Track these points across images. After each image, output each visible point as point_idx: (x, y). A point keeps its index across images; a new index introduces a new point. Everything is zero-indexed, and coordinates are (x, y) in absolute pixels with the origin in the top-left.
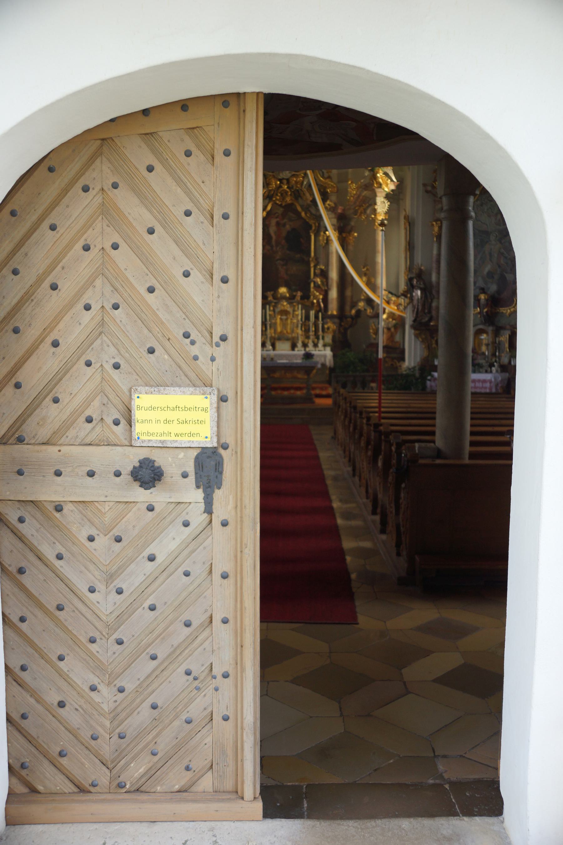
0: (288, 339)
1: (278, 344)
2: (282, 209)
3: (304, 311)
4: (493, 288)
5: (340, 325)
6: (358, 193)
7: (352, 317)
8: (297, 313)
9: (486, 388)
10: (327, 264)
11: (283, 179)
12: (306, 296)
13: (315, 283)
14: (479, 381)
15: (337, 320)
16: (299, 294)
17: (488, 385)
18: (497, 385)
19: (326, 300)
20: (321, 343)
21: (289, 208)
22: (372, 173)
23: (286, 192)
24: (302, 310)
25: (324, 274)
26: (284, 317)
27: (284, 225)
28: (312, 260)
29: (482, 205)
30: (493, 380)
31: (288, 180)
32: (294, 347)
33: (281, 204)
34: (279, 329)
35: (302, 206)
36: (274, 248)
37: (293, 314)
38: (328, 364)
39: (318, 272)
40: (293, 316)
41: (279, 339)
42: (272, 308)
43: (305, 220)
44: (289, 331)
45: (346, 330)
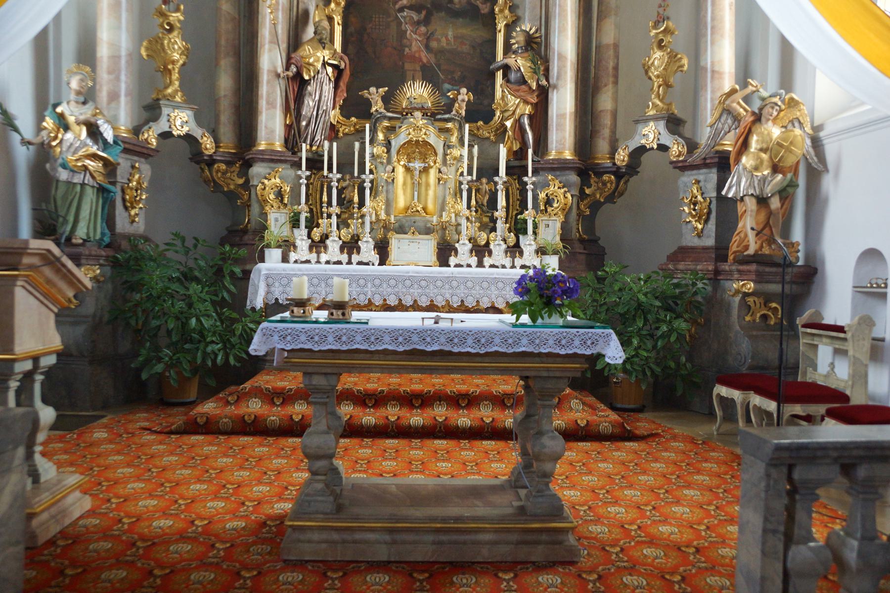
0: (428, 231)
1: (398, 245)
3: (476, 149)
5: (582, 195)
7: (618, 173)
8: (456, 152)
10: (546, 21)
13: (506, 68)
15: (574, 178)
16: (464, 95)
20: (528, 244)
24: (471, 146)
26: (417, 165)
28: (501, 11)
32: (445, 253)
34: (401, 202)
37: (445, 155)
39: (518, 40)
40: (445, 162)
41: (401, 230)
42: (381, 136)
44: (430, 206)
45: (596, 206)
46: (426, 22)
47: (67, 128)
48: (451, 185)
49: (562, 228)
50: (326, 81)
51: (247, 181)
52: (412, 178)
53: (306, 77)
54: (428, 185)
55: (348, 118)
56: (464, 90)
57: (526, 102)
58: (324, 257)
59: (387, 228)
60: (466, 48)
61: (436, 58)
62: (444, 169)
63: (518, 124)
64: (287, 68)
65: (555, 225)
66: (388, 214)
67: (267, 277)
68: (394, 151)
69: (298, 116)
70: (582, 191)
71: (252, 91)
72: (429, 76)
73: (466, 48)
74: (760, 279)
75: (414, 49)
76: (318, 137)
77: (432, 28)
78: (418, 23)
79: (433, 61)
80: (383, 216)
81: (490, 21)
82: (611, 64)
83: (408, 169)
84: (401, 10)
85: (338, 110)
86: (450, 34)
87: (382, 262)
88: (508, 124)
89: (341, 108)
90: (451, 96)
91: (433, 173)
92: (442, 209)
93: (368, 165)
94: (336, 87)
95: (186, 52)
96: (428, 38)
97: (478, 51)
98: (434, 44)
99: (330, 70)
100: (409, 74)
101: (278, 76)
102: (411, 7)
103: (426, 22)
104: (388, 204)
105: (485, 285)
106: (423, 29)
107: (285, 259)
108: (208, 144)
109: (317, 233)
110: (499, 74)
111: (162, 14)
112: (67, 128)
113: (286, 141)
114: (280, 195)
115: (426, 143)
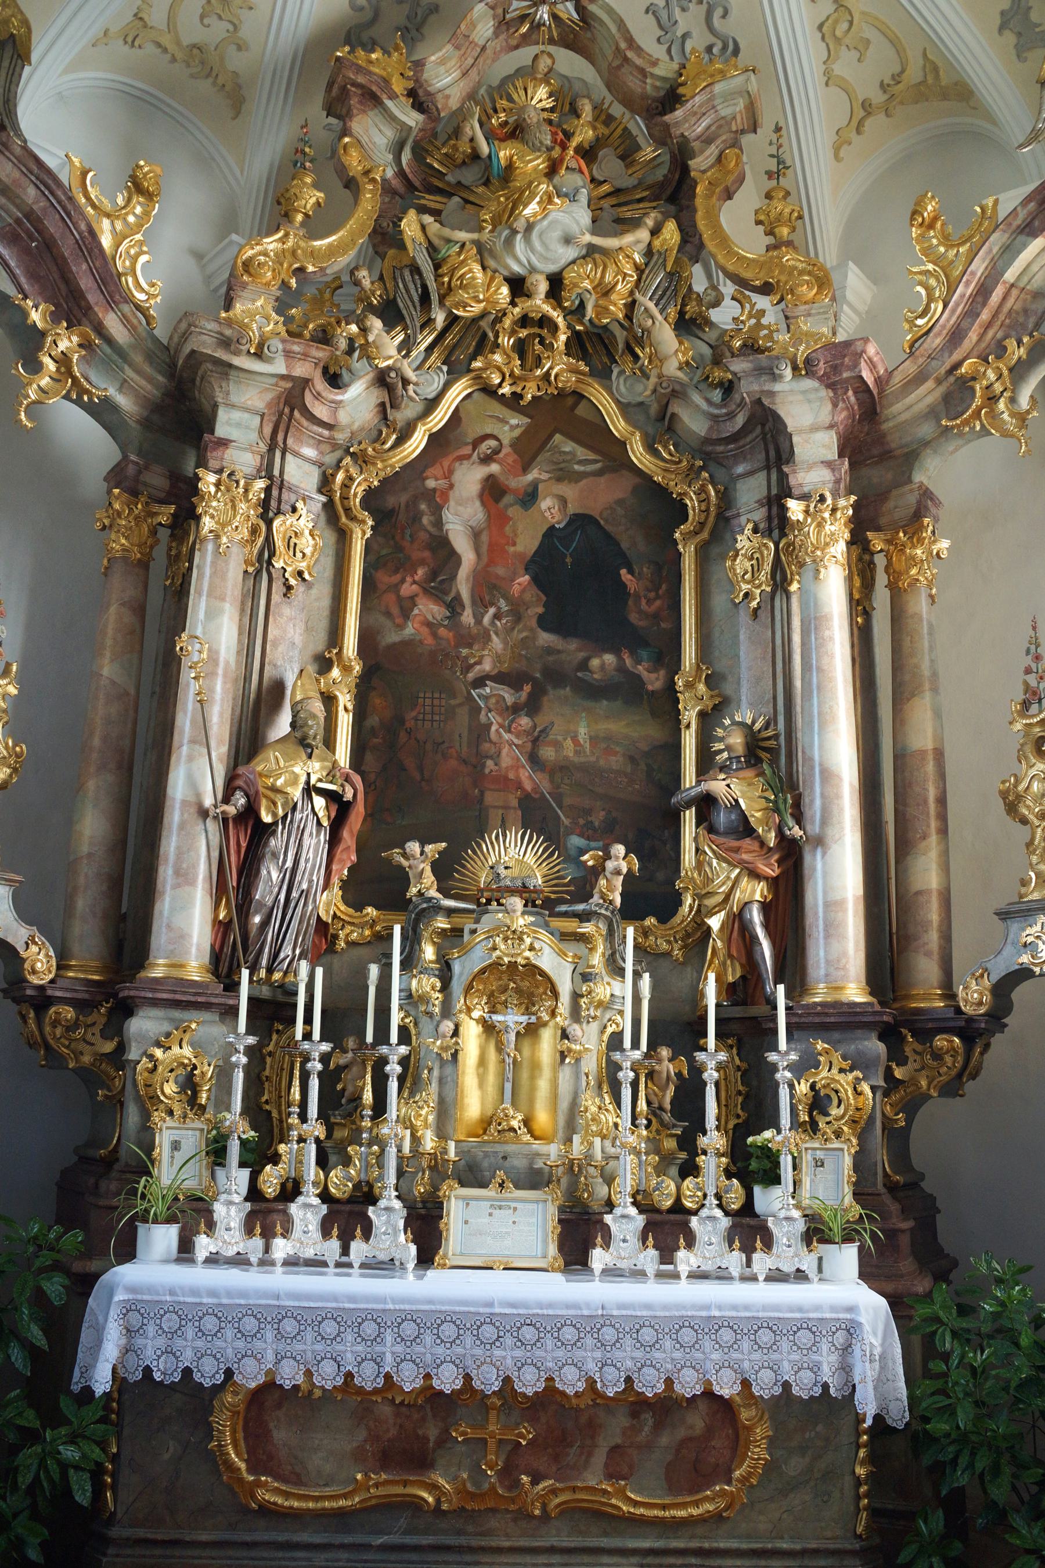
5: (892, 1083)
13: (706, 804)
24: (637, 975)
26: (513, 1019)
27: (530, 497)
28: (690, 686)
33: (517, 396)
35: (625, 408)
36: (467, 617)
37: (576, 996)
38: (868, 1405)
42: (429, 952)
43: (647, 478)
44: (542, 1118)
45: (912, 1107)
46: (532, 706)
48: (591, 1064)
49: (856, 1167)
50: (311, 826)
51: (122, 1048)
52: (500, 1048)
53: (267, 819)
54: (535, 1066)
55: (358, 906)
56: (620, 849)
57: (755, 875)
58: (281, 1248)
59: (437, 1167)
60: (616, 762)
61: (552, 781)
62: (575, 1030)
63: (738, 922)
64: (226, 800)
66: (442, 1135)
67: (129, 1308)
68: (457, 986)
69: (244, 905)
70: (889, 1075)
73: (616, 762)
75: (506, 761)
76: (287, 951)
77: (542, 720)
78: (515, 709)
80: (429, 1143)
82: (932, 793)
83: (489, 1028)
84: (480, 682)
85: (336, 891)
86: (583, 731)
87: (426, 1259)
88: (715, 922)
89: (345, 886)
90: (590, 863)
91: (547, 1037)
92: (571, 1128)
93: (396, 1018)
94: (334, 841)
96: (537, 739)
97: (643, 766)
98: (548, 753)
99: (319, 802)
100: (495, 816)
101: (204, 814)
102: (500, 678)
103: (532, 706)
104: (445, 1110)
105: (687, 1336)
106: (525, 721)
107: (185, 1249)
109: (271, 1179)
110: (689, 817)
113: (216, 957)
114: (190, 1085)
115: (533, 970)
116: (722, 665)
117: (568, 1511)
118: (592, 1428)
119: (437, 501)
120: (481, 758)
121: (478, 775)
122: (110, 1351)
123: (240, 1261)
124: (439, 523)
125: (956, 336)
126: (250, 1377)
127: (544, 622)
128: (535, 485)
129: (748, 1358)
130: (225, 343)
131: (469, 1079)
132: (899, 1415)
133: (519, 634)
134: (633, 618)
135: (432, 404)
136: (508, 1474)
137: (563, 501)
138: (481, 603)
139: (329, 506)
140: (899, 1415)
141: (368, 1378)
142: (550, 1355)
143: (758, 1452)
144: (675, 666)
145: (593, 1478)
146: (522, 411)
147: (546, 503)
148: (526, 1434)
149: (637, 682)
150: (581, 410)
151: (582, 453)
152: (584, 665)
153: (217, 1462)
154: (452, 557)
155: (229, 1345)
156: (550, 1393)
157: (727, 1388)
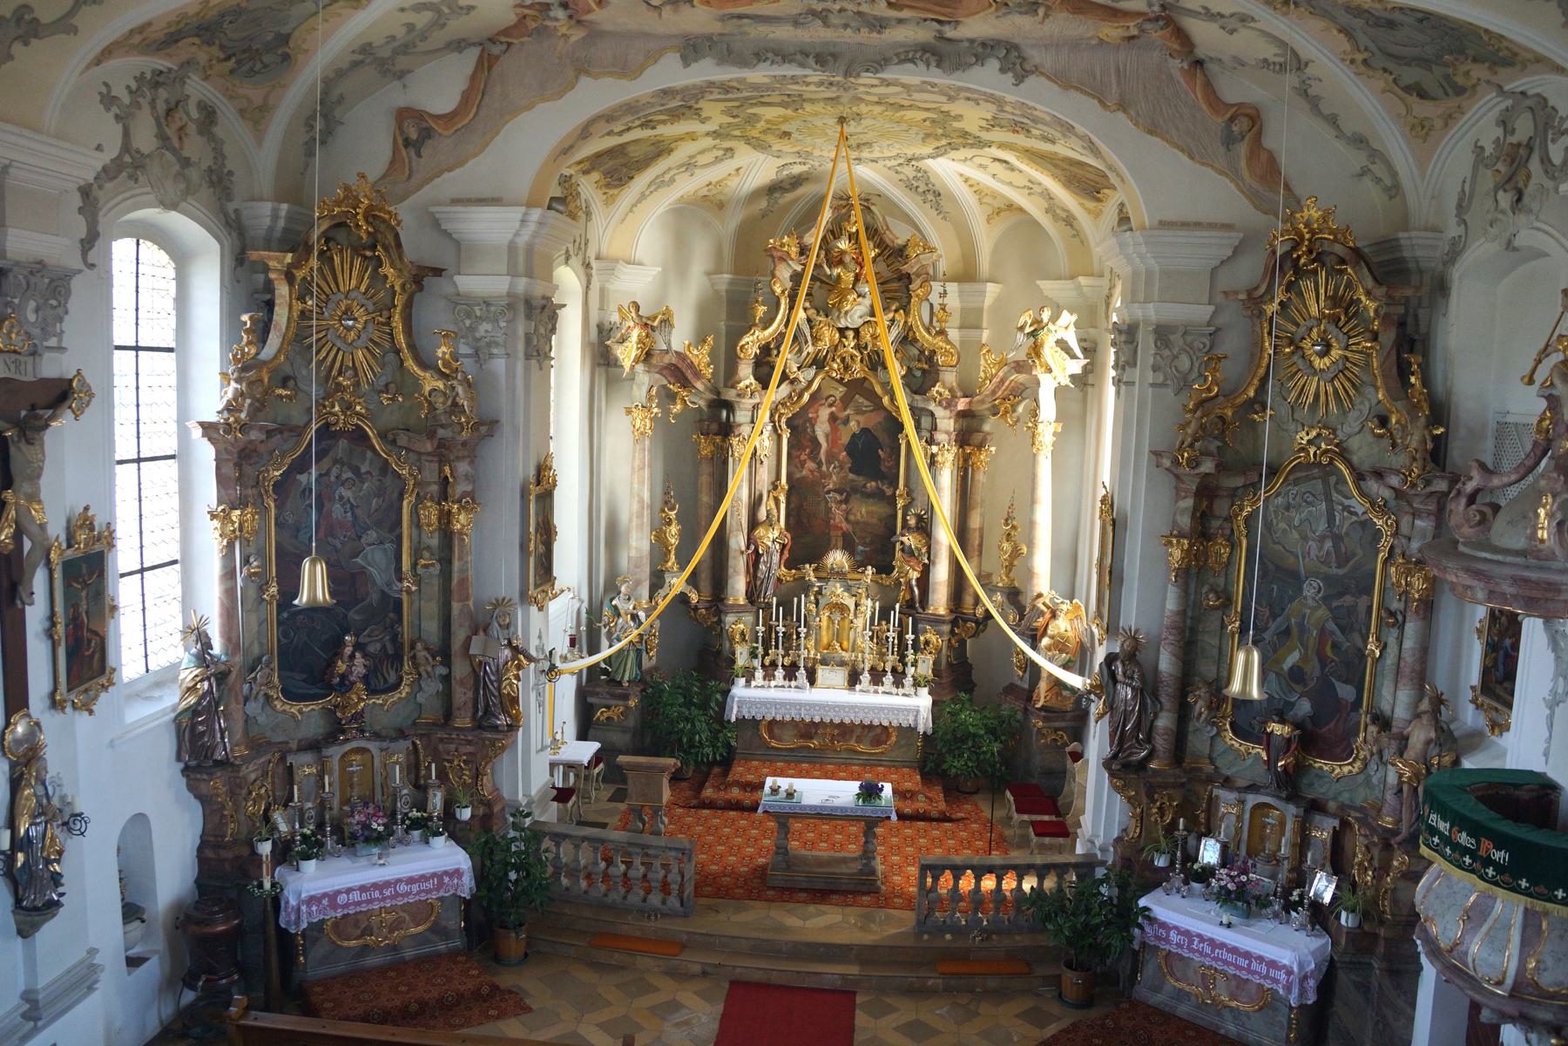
0: (842, 664)
1: (822, 672)
2: (842, 389)
4: (1304, 707)
6: (1001, 374)
7: (977, 622)
9: (1276, 981)
11: (847, 328)
12: (884, 568)
14: (1260, 959)
17: (1282, 976)
18: (1304, 979)
19: (924, 581)
21: (857, 388)
22: (1032, 339)
23: (852, 357)
25: (925, 527)
27: (846, 421)
29: (1288, 508)
30: (1295, 969)
31: (857, 331)
32: (853, 680)
33: (842, 379)
36: (824, 468)
38: (921, 729)
39: (912, 522)
40: (856, 616)
41: (824, 662)
46: (846, 501)
47: (619, 615)
49: (934, 663)
58: (773, 683)
60: (874, 521)
64: (748, 548)
65: (930, 659)
68: (821, 606)
69: (755, 576)
71: (722, 551)
72: (849, 547)
73: (874, 521)
74: (1045, 719)
78: (841, 502)
79: (851, 529)
81: (892, 501)
82: (977, 542)
84: (828, 492)
95: (681, 534)
96: (847, 513)
98: (852, 518)
100: (833, 542)
101: (742, 553)
103: (846, 501)
106: (844, 506)
108: (694, 597)
111: (664, 511)
112: (619, 615)
114: (743, 634)
116: (913, 486)
117: (846, 750)
118: (852, 731)
119: (813, 422)
120: (830, 518)
121: (828, 522)
122: (735, 711)
123: (763, 687)
124: (814, 431)
125: (994, 392)
126: (769, 718)
127: (851, 470)
128: (848, 416)
129: (891, 717)
130: (739, 395)
131: (824, 633)
132: (930, 732)
133: (842, 475)
134: (883, 468)
135: (810, 383)
136: (832, 741)
137: (858, 423)
138: (829, 463)
139: (774, 427)
140: (930, 732)
141: (797, 719)
142: (842, 714)
143: (894, 739)
144: (897, 487)
145: (852, 742)
146: (844, 385)
147: (852, 423)
148: (836, 732)
149: (883, 492)
150: (866, 384)
151: (866, 403)
152: (865, 486)
153: (761, 737)
154: (818, 445)
155: (764, 710)
156: (842, 724)
157: (886, 724)
